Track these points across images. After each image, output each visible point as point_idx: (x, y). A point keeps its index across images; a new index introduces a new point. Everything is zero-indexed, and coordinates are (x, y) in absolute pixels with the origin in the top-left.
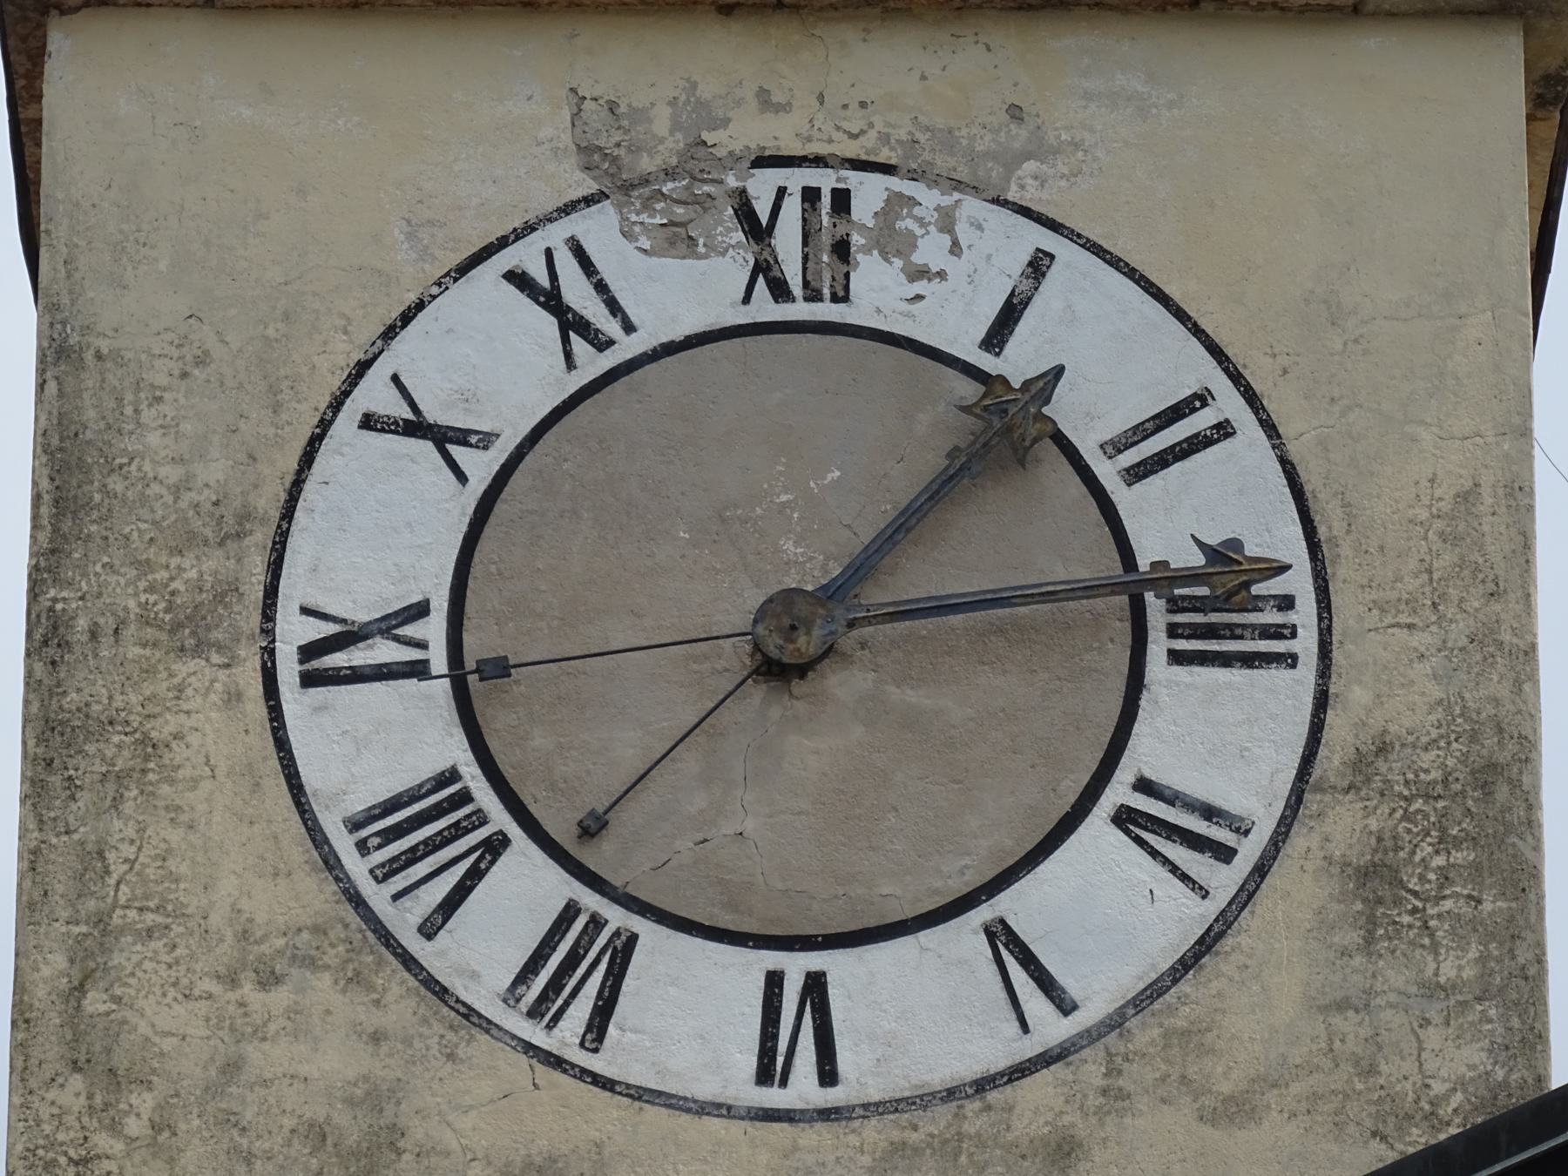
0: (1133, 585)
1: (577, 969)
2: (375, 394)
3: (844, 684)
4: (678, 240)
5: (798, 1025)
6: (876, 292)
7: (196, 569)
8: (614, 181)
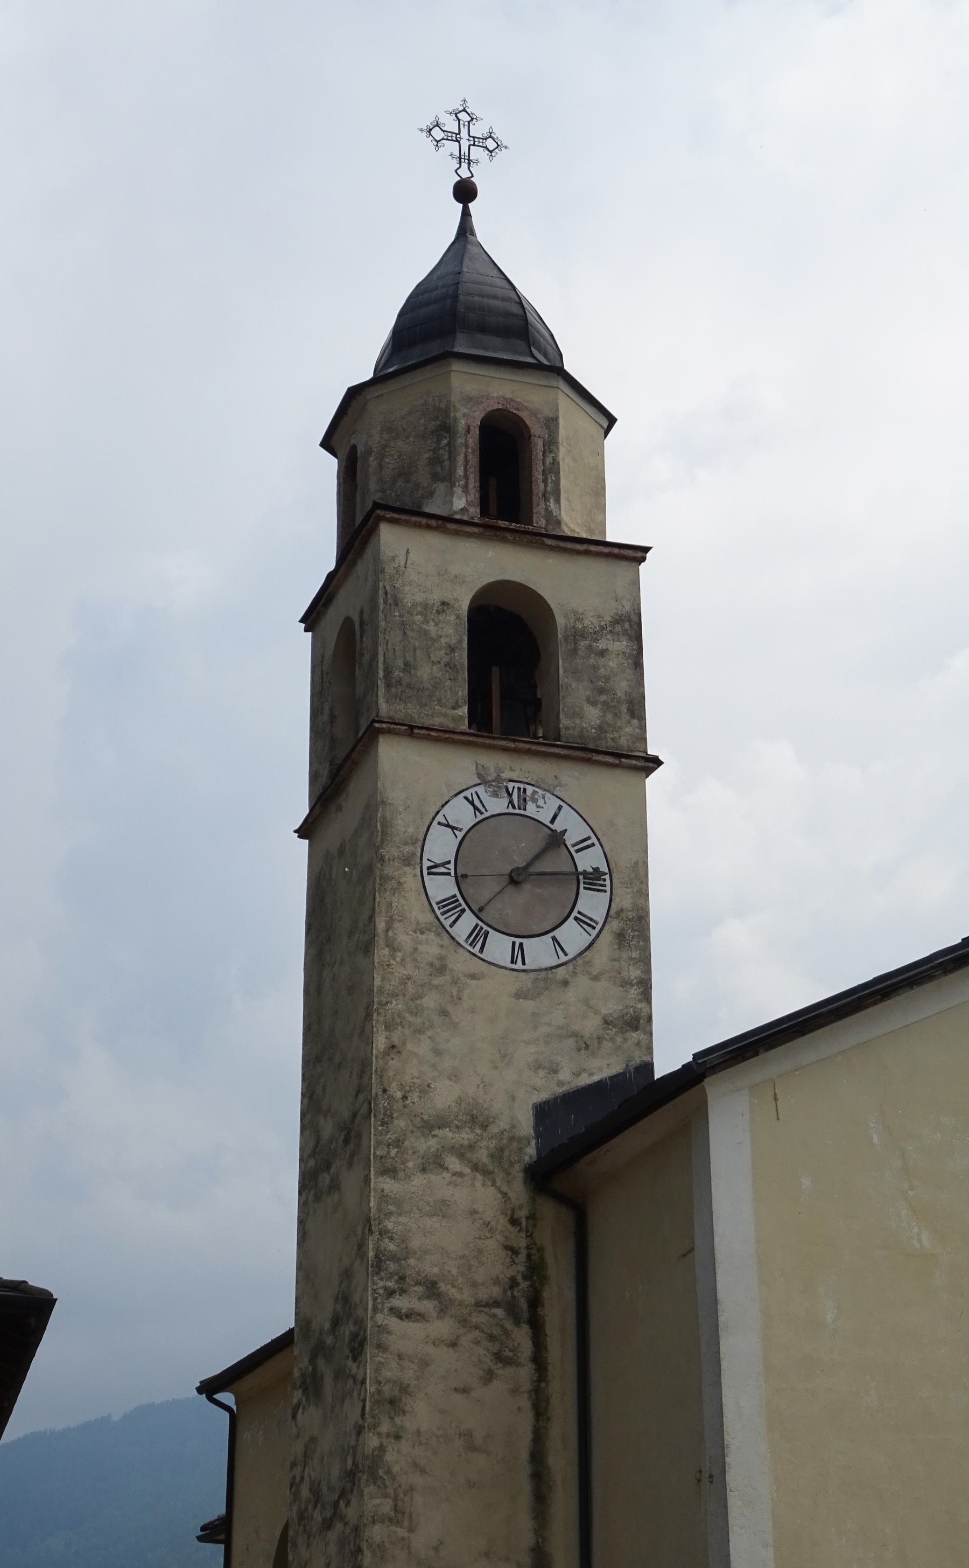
0: (577, 874)
2: (440, 818)
3: (527, 887)
4: (495, 794)
5: (518, 952)
6: (531, 810)
7: (407, 849)
8: (484, 782)
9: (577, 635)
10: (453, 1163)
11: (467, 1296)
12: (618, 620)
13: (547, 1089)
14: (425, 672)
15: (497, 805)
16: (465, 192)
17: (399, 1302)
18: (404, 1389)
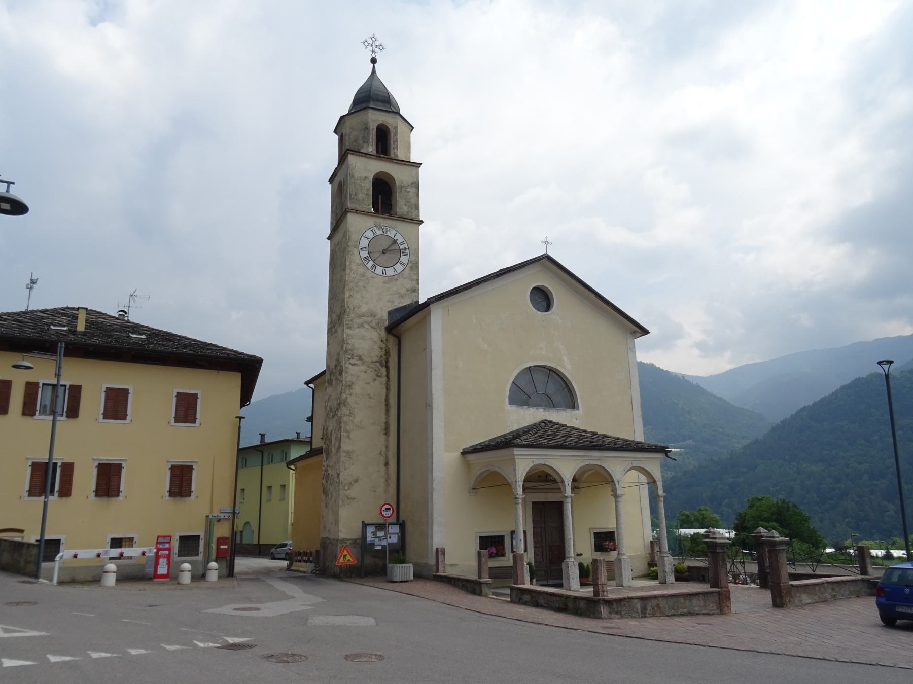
1: (374, 267)
6: (388, 234)
8: (376, 226)
9: (402, 187)
10: (366, 326)
11: (369, 360)
12: (413, 183)
13: (392, 307)
14: (360, 196)
15: (379, 232)
16: (374, 61)
17: (352, 361)
18: (352, 383)
